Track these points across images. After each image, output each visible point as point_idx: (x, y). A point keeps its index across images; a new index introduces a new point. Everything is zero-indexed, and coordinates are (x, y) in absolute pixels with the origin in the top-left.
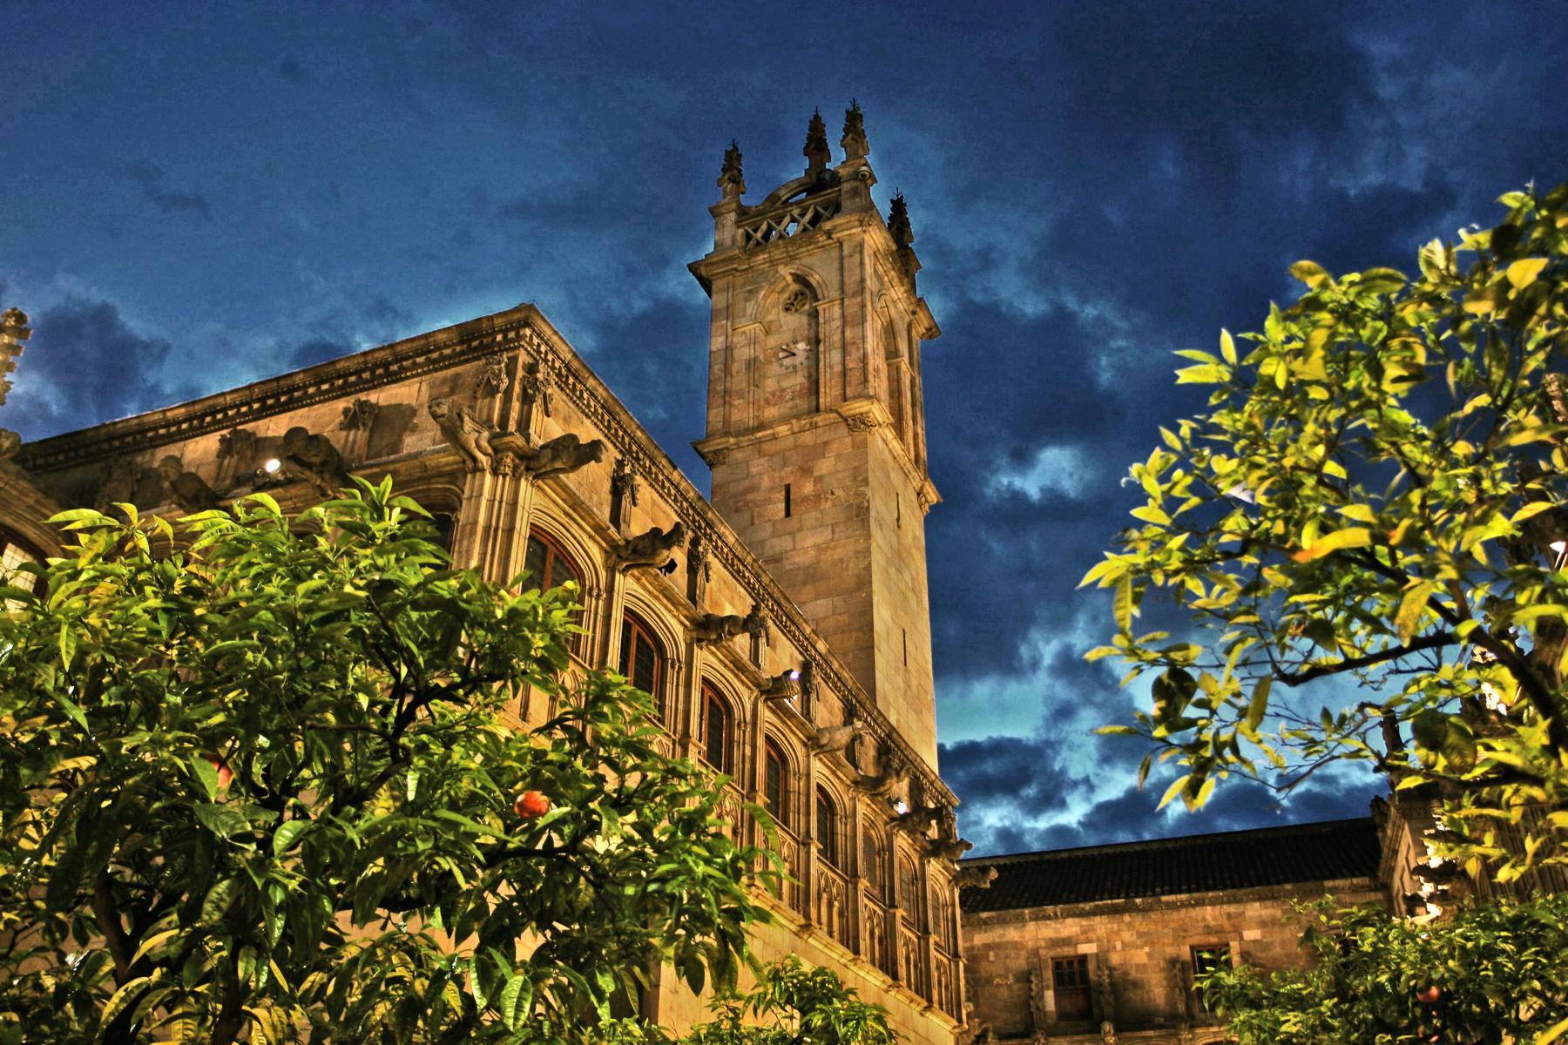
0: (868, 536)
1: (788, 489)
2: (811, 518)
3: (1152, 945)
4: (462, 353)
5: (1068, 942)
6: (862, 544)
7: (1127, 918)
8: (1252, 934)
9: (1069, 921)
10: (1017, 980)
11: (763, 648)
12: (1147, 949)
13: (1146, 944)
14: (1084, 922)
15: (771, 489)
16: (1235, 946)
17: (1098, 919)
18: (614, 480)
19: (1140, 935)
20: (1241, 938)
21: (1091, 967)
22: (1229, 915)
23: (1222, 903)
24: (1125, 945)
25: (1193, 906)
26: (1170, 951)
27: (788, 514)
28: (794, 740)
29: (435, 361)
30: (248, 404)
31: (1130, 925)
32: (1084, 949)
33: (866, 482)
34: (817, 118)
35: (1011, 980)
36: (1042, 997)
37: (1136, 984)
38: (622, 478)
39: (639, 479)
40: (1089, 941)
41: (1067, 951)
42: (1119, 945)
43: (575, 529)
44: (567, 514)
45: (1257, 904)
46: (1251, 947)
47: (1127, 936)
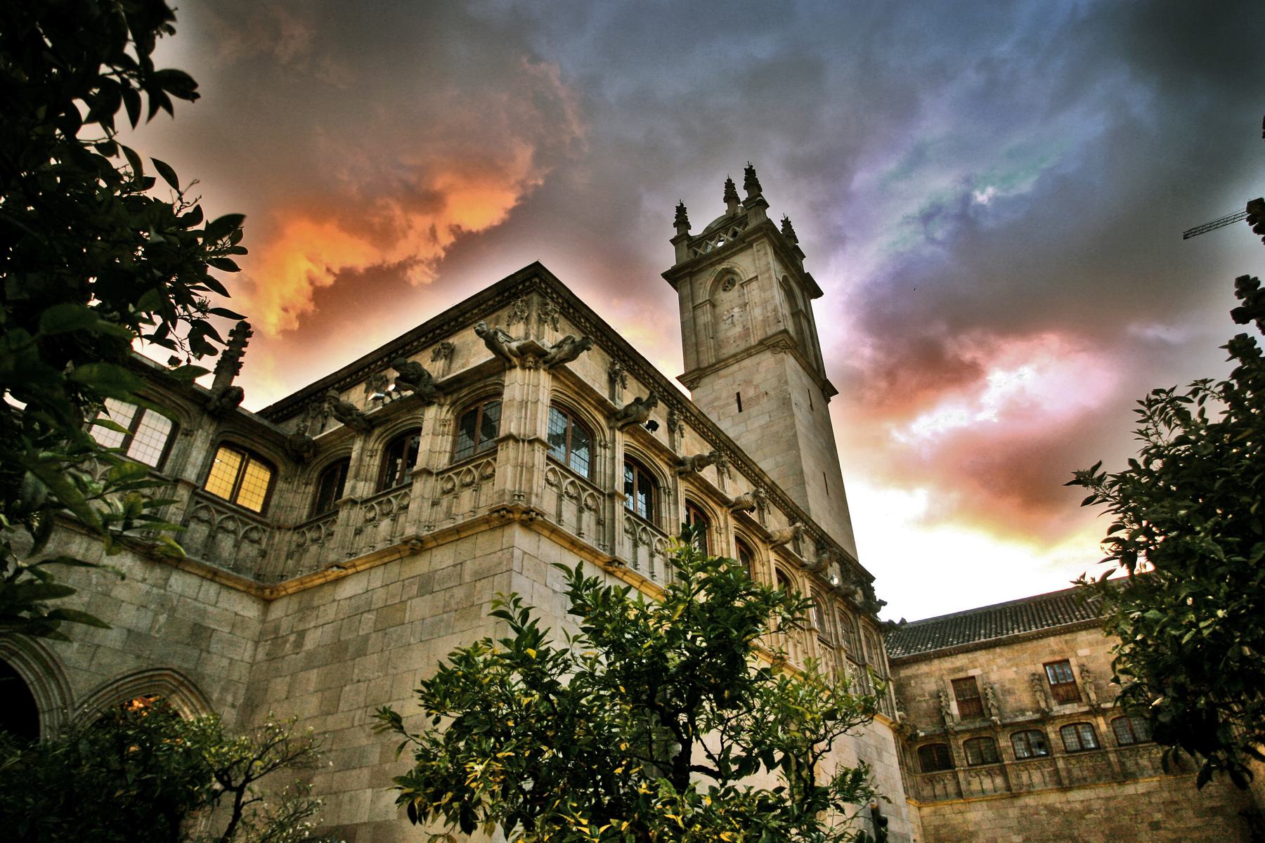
0: (793, 415)
1: (738, 394)
2: (754, 411)
3: (1017, 665)
4: (500, 301)
5: (961, 669)
6: (789, 421)
7: (998, 650)
8: (1083, 652)
9: (960, 656)
10: (931, 695)
11: (727, 481)
14: (970, 656)
15: (728, 398)
16: (1073, 661)
17: (979, 653)
18: (610, 375)
19: (1009, 660)
20: (1077, 656)
21: (979, 683)
22: (1066, 642)
23: (1060, 634)
24: (1000, 668)
26: (1031, 668)
27: (740, 410)
28: (757, 540)
29: (484, 310)
30: (381, 359)
31: (1001, 655)
32: (971, 673)
33: (786, 382)
34: (729, 180)
35: (927, 697)
37: (1009, 692)
38: (616, 373)
39: (626, 373)
41: (962, 675)
42: (995, 668)
43: (585, 404)
44: (577, 393)
45: (1084, 633)
46: (1084, 661)
47: (1000, 661)
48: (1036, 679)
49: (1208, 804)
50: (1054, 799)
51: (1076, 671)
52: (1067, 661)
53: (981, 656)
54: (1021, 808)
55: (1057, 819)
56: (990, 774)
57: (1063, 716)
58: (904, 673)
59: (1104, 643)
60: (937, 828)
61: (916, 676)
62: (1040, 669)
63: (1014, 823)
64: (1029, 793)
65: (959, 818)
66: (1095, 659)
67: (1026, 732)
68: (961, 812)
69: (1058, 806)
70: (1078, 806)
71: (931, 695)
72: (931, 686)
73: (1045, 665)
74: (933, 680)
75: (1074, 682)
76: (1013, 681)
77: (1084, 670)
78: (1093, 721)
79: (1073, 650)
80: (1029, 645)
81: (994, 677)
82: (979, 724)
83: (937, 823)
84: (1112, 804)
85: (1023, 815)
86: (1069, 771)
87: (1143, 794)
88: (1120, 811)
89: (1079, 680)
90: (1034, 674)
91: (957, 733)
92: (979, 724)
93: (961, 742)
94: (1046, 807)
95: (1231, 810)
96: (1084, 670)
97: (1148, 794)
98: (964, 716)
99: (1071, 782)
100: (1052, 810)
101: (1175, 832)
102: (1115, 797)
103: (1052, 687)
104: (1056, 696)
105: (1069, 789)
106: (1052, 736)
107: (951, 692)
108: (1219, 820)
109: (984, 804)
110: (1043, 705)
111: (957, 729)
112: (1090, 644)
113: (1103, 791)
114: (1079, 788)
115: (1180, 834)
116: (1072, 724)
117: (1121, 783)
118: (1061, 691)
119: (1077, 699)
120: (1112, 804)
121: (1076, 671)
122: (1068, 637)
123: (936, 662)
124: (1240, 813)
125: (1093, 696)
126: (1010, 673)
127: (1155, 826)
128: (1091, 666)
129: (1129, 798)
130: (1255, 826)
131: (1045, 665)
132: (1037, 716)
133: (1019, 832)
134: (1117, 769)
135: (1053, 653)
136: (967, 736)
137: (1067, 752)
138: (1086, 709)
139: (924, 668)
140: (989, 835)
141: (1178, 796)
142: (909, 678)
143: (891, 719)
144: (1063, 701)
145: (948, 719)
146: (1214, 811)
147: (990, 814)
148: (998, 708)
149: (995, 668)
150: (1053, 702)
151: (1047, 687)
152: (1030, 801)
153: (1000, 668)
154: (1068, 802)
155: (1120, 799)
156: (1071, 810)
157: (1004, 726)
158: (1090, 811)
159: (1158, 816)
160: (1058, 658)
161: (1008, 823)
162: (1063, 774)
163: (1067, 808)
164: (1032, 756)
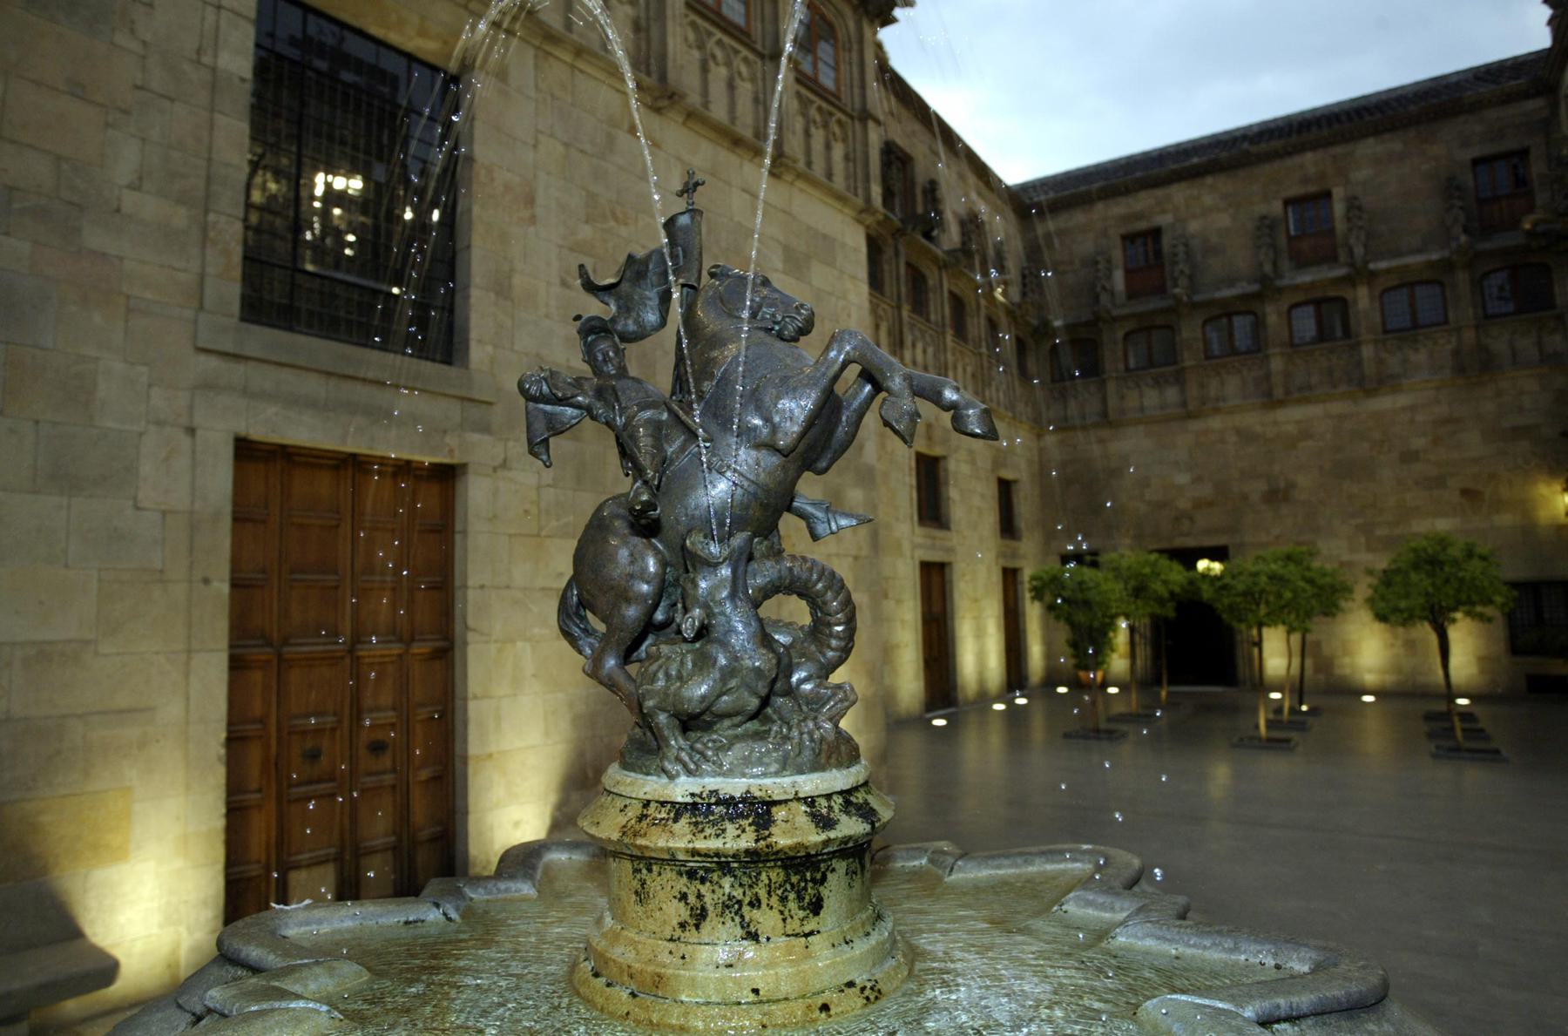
5: (1139, 216)
7: (1209, 180)
9: (1143, 195)
14: (1159, 192)
16: (1338, 193)
26: (1260, 209)
36: (1109, 277)
40: (1164, 212)
41: (1142, 225)
45: (1371, 140)
48: (1267, 226)
50: (1252, 420)
51: (1339, 208)
52: (1328, 195)
53: (1179, 193)
56: (1158, 383)
57: (1296, 288)
61: (1061, 233)
62: (1277, 207)
64: (1217, 410)
69: (1259, 429)
70: (1291, 429)
72: (1086, 246)
75: (1332, 231)
78: (1347, 293)
80: (1267, 168)
82: (1154, 304)
87: (1404, 409)
89: (1340, 226)
90: (1263, 218)
91: (1115, 319)
92: (1154, 304)
93: (1120, 334)
94: (1238, 431)
96: (1353, 205)
97: (1413, 408)
98: (1132, 294)
99: (1288, 392)
100: (1246, 436)
105: (1281, 403)
107: (1117, 254)
109: (1141, 428)
110: (1268, 268)
111: (1115, 313)
113: (1337, 407)
114: (1299, 402)
117: (1370, 393)
119: (1331, 258)
122: (1338, 150)
123: (1100, 206)
125: (1359, 251)
126: (1223, 220)
127: (1409, 457)
132: (1255, 288)
135: (1305, 180)
136: (1130, 325)
137: (1292, 345)
139: (1078, 217)
143: (860, 201)
144: (1301, 263)
145: (1104, 299)
146: (1517, 433)
148: (1191, 278)
150: (1285, 265)
151: (1282, 241)
152: (1215, 423)
154: (1275, 423)
157: (1195, 306)
159: (1419, 443)
160: (1312, 189)
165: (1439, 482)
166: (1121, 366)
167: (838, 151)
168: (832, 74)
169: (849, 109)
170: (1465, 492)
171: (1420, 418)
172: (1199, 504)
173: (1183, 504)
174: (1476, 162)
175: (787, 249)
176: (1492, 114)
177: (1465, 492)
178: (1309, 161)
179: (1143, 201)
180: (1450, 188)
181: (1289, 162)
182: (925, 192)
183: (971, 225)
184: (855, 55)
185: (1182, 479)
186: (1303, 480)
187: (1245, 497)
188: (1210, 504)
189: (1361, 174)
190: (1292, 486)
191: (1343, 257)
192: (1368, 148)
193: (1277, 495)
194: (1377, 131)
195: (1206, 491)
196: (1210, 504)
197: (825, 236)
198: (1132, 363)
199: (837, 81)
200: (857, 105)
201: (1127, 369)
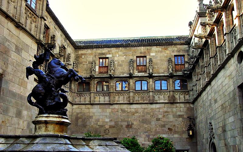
3: (126, 56)
5: (103, 54)
7: (121, 48)
8: (152, 54)
10: (89, 62)
12: (125, 57)
13: (125, 55)
14: (109, 49)
17: (113, 48)
19: (123, 53)
20: (150, 55)
23: (146, 46)
24: (119, 56)
25: (139, 46)
26: (131, 57)
31: (121, 51)
32: (107, 56)
35: (88, 63)
36: (95, 67)
37: (121, 65)
40: (110, 54)
41: (104, 56)
42: (117, 55)
46: (152, 58)
47: (120, 53)
49: (179, 113)
52: (146, 57)
53: (114, 50)
54: (112, 109)
55: (124, 114)
58: (81, 52)
59: (161, 52)
60: (78, 114)
63: (108, 114)
65: (87, 111)
66: (156, 58)
67: (122, 81)
68: (89, 108)
70: (133, 110)
71: (89, 62)
72: (90, 59)
73: (137, 57)
74: (92, 56)
75: (146, 65)
76: (123, 61)
77: (151, 60)
79: (149, 53)
80: (133, 48)
81: (116, 59)
83: (78, 112)
84: (146, 110)
85: (112, 112)
86: (134, 97)
88: (148, 113)
89: (148, 65)
90: (131, 60)
93: (96, 82)
94: (122, 110)
95: (185, 116)
96: (151, 60)
99: (133, 101)
100: (123, 111)
101: (164, 122)
102: (147, 108)
103: (137, 66)
104: (138, 69)
106: (131, 83)
108: (181, 119)
112: (156, 52)
115: (166, 123)
116: (141, 79)
118: (140, 68)
119: (145, 72)
120: (146, 110)
121: (148, 61)
122: (149, 48)
123: (95, 50)
124: (188, 117)
125: (151, 71)
126: (123, 58)
127: (158, 120)
128: (154, 60)
129: (152, 109)
130: (191, 122)
131: (137, 57)
132: (128, 75)
133: (110, 118)
134: (151, 98)
138: (147, 75)
139: (89, 51)
140: (97, 117)
141: (169, 110)
142: (82, 54)
145: (93, 73)
146: (180, 116)
147: (100, 110)
148: (114, 71)
149: (117, 55)
151: (135, 66)
153: (119, 56)
155: (149, 109)
156: (130, 111)
158: (137, 112)
159: (160, 116)
160: (143, 55)
161: (106, 114)
162: (131, 98)
163: (129, 110)
164: (122, 90)
165: (164, 126)
166: (96, 90)
167: (33, 25)
168: (34, 5)
169: (38, 15)
170: (169, 129)
171: (161, 111)
172: (111, 127)
173: (107, 127)
174: (175, 56)
175: (16, 46)
176: (179, 46)
177: (169, 129)
178: (142, 49)
179: (105, 50)
180: (170, 61)
181: (138, 48)
182: (51, 38)
183: (63, 48)
184: (41, 3)
185: (107, 120)
186: (135, 123)
187: (122, 126)
188: (114, 127)
189: (152, 54)
190: (132, 124)
191: (148, 72)
192: (154, 48)
193: (129, 126)
194: (157, 45)
195: (113, 124)
196: (114, 127)
197: (27, 45)
198: (98, 90)
199: (36, 7)
200: (40, 14)
201: (97, 91)
